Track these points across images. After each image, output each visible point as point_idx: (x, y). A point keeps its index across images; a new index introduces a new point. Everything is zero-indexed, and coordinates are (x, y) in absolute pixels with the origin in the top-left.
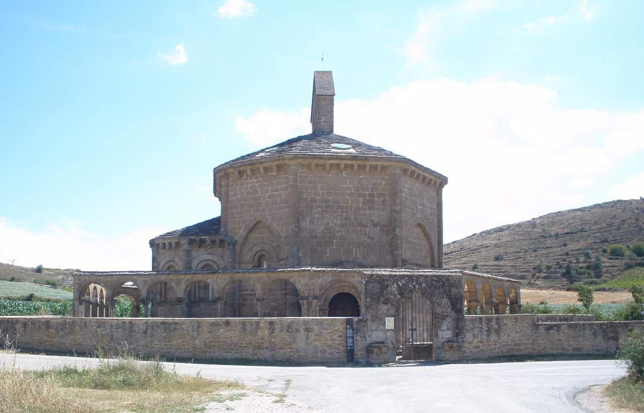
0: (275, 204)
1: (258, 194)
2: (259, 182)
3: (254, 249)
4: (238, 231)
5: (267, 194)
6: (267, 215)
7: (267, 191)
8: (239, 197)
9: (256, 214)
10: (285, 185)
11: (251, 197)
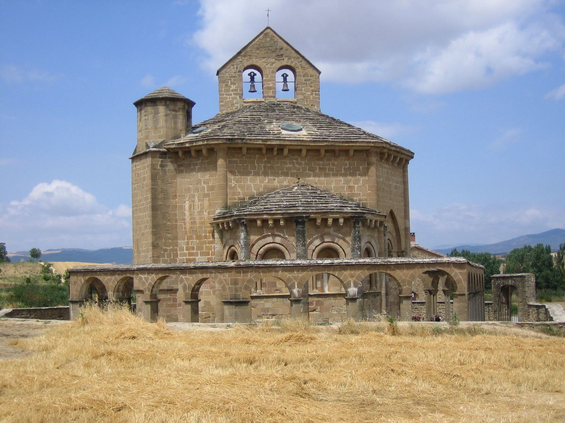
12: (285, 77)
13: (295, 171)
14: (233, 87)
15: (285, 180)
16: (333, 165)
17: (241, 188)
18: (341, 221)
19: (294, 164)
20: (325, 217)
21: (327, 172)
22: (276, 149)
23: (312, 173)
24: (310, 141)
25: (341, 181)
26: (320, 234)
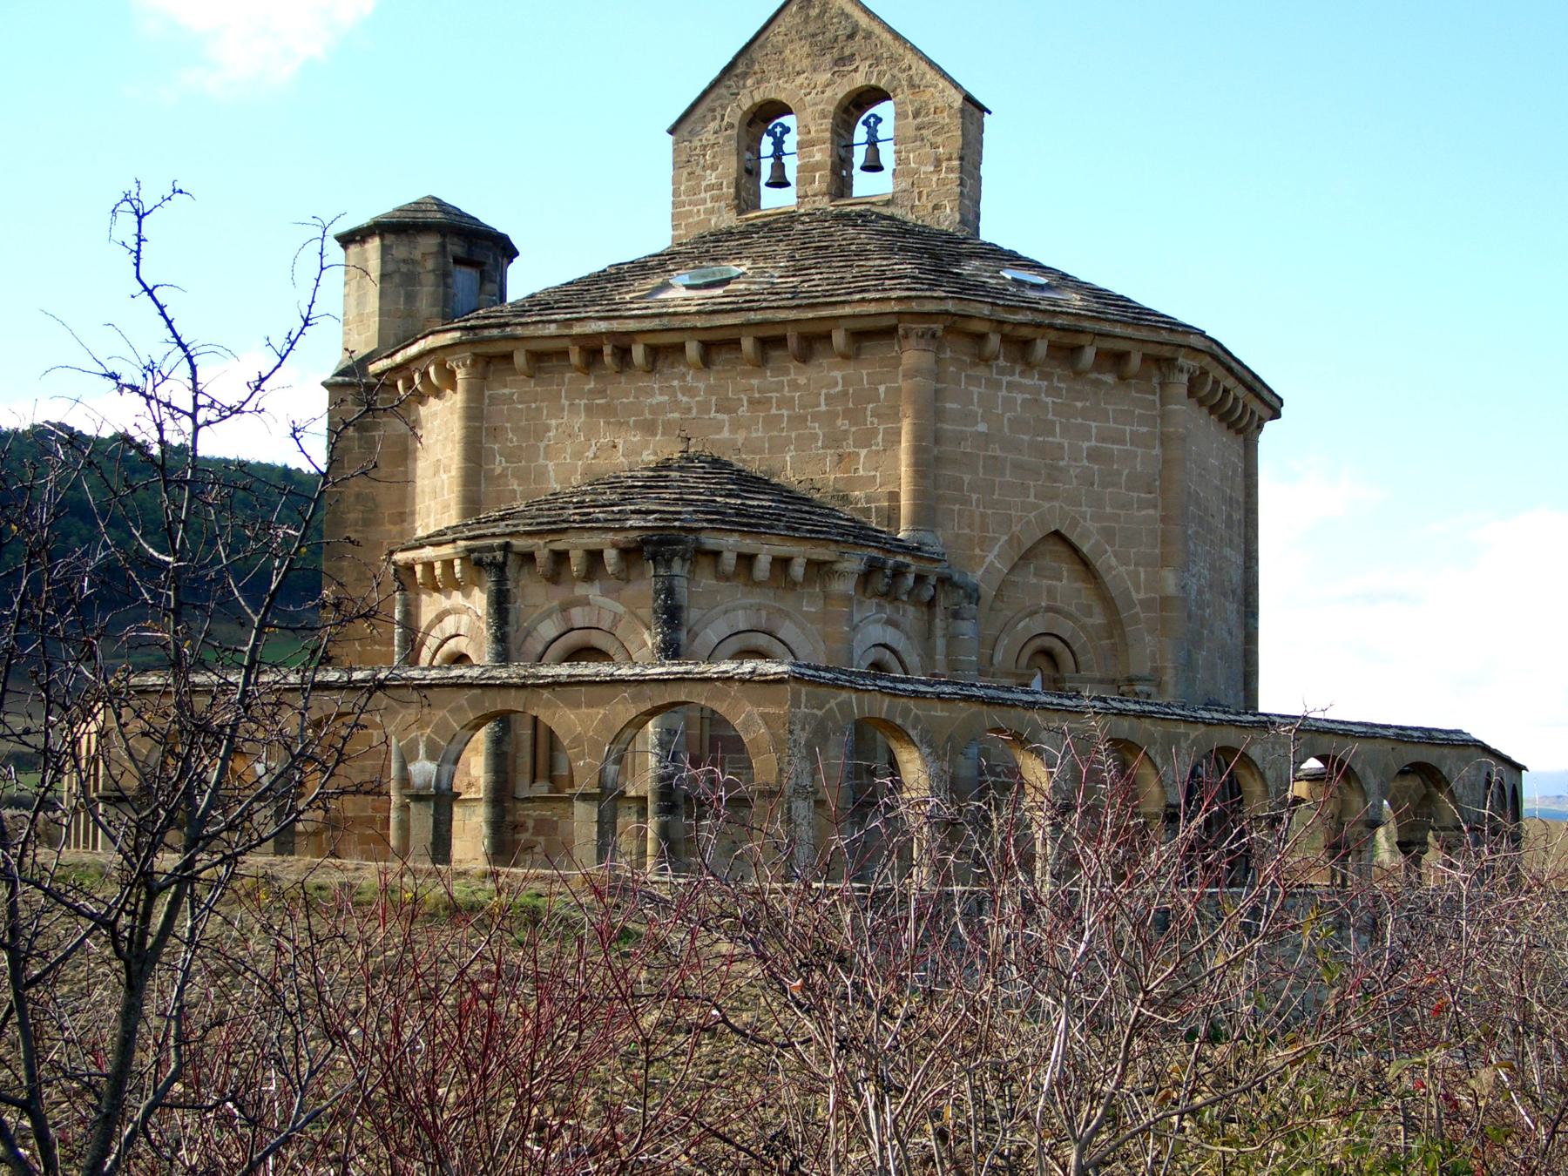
0: (1113, 485)
1: (1052, 433)
2: (1055, 392)
3: (1021, 624)
4: (977, 551)
5: (1086, 445)
6: (1085, 519)
7: (1085, 433)
8: (982, 427)
9: (1047, 505)
10: (1144, 429)
11: (1026, 438)
12: (873, 125)
13: (676, 415)
14: (712, 177)
15: (646, 447)
16: (794, 386)
17: (518, 478)
18: (610, 555)
19: (671, 391)
20: (559, 546)
21: (774, 411)
22: (607, 350)
23: (725, 417)
24: (698, 313)
25: (814, 437)
26: (555, 603)
